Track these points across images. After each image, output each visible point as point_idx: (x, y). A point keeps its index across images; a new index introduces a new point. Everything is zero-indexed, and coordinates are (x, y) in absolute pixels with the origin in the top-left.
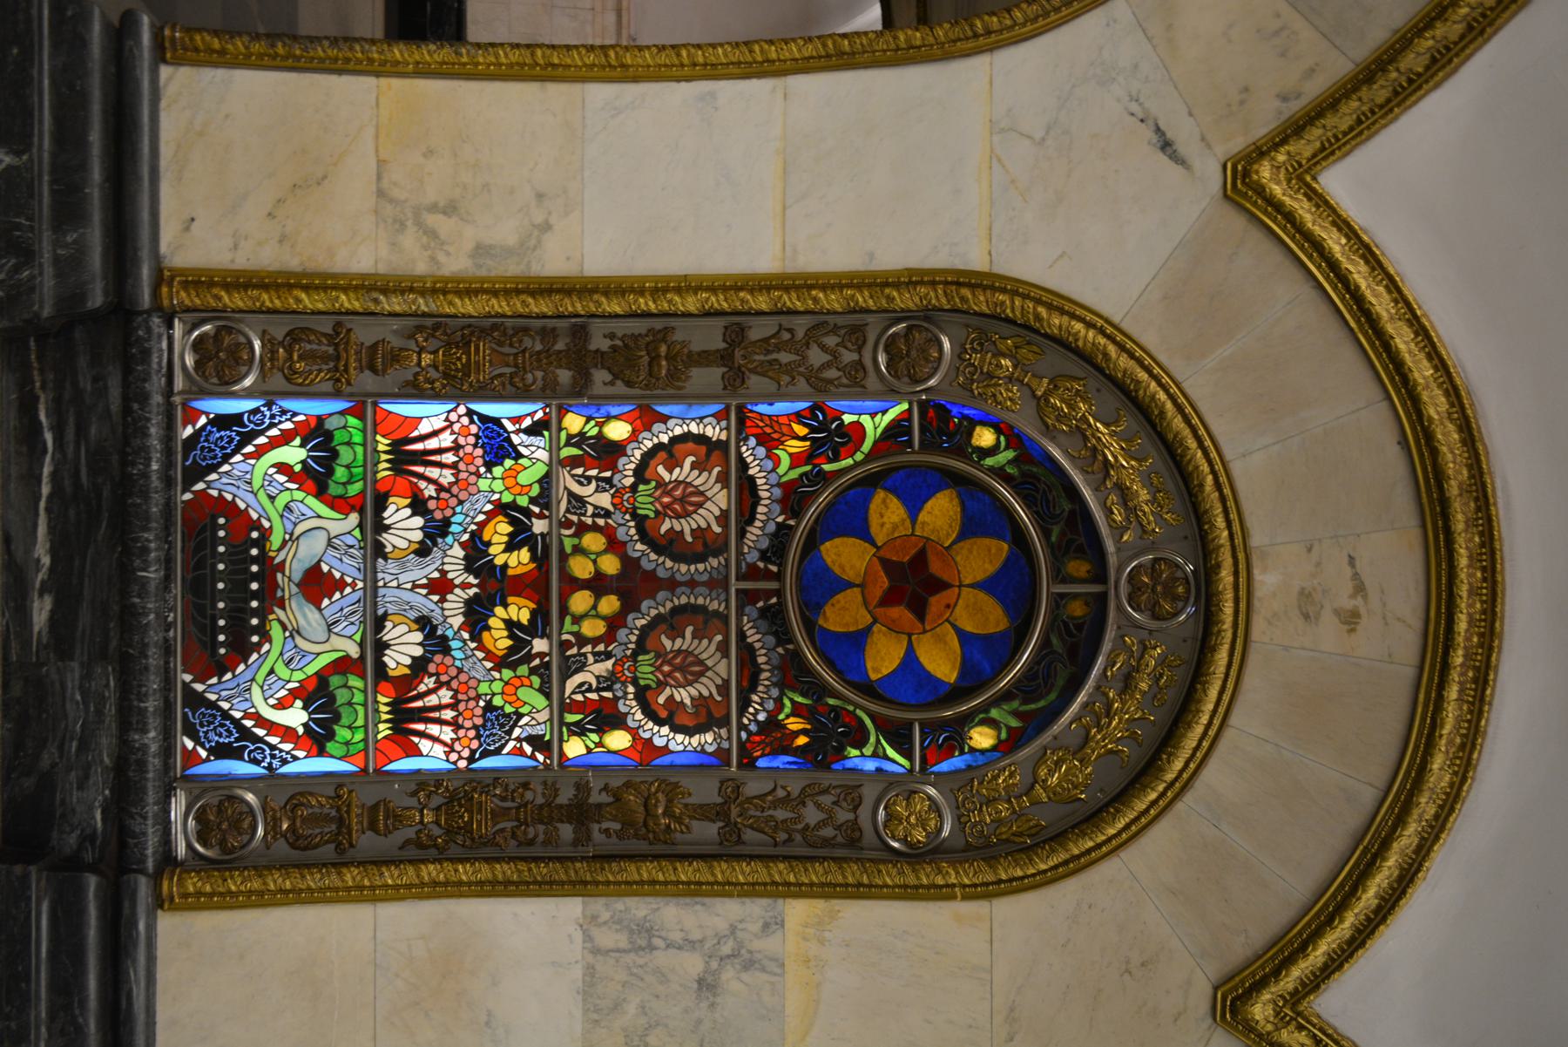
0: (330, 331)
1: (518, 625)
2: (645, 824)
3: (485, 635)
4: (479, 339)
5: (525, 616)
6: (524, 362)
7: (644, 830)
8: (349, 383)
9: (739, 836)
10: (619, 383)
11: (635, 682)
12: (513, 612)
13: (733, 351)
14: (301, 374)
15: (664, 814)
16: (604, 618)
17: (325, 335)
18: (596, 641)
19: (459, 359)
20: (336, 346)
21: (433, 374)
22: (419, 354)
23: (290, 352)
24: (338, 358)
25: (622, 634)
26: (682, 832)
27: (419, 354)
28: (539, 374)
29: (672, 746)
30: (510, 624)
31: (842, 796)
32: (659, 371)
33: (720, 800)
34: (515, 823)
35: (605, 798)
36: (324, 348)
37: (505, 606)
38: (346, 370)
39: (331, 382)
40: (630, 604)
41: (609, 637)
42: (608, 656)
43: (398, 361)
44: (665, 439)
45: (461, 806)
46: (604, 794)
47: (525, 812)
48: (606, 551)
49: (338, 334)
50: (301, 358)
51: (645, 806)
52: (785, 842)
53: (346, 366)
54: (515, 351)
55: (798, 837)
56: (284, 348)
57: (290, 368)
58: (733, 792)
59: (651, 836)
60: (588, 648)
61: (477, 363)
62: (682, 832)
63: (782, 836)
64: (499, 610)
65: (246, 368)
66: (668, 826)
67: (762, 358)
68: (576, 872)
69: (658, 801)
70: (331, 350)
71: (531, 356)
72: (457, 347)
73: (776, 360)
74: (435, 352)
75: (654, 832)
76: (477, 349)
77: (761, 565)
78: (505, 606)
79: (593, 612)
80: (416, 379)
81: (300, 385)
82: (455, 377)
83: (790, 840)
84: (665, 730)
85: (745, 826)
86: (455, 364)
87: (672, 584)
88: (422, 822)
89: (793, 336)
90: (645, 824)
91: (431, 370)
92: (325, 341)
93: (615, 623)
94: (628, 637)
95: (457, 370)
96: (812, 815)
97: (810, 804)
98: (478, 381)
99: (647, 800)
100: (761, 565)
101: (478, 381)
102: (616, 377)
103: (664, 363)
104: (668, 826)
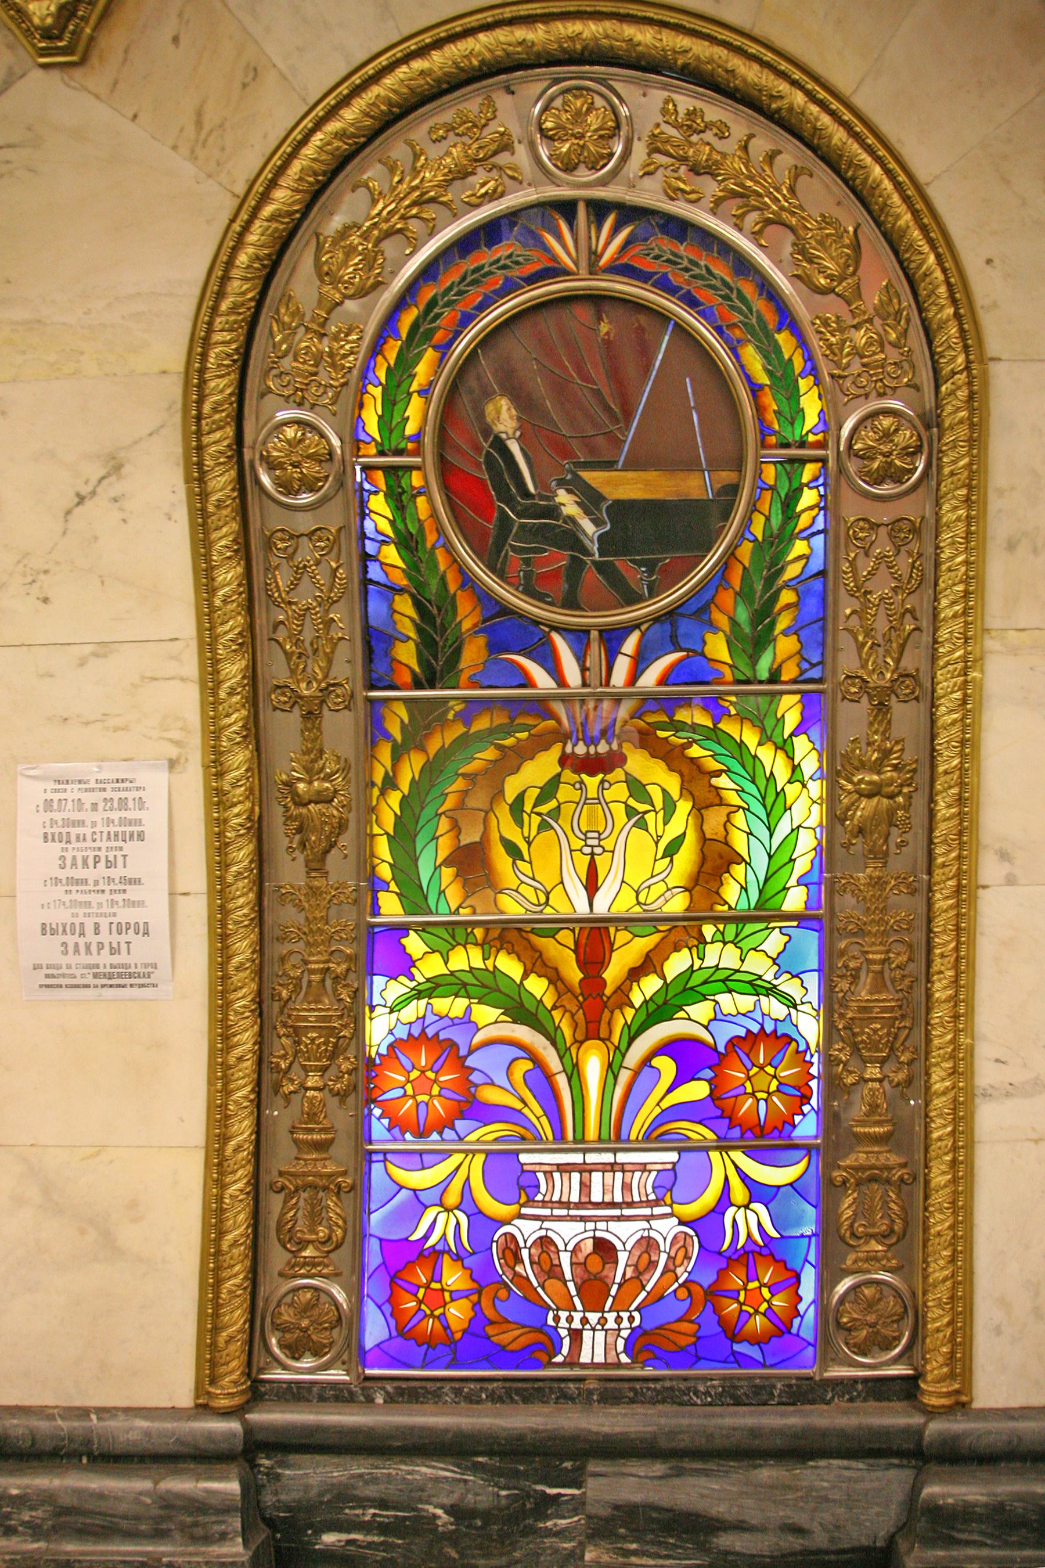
0: (281, 1197)
8: (345, 1173)
14: (332, 1231)
17: (285, 1202)
19: (313, 1040)
20: (297, 1190)
21: (332, 1073)
22: (307, 1089)
24: (314, 1187)
27: (307, 1089)
43: (315, 1114)
45: (864, 1033)
54: (306, 974)
57: (324, 1243)
61: (319, 1019)
67: (309, 662)
73: (312, 644)
76: (305, 1019)
80: (338, 1094)
82: (336, 1045)
86: (319, 1046)
88: (880, 1081)
89: (282, 622)
91: (328, 1074)
92: (294, 1201)
98: (341, 1017)
101: (341, 1017)
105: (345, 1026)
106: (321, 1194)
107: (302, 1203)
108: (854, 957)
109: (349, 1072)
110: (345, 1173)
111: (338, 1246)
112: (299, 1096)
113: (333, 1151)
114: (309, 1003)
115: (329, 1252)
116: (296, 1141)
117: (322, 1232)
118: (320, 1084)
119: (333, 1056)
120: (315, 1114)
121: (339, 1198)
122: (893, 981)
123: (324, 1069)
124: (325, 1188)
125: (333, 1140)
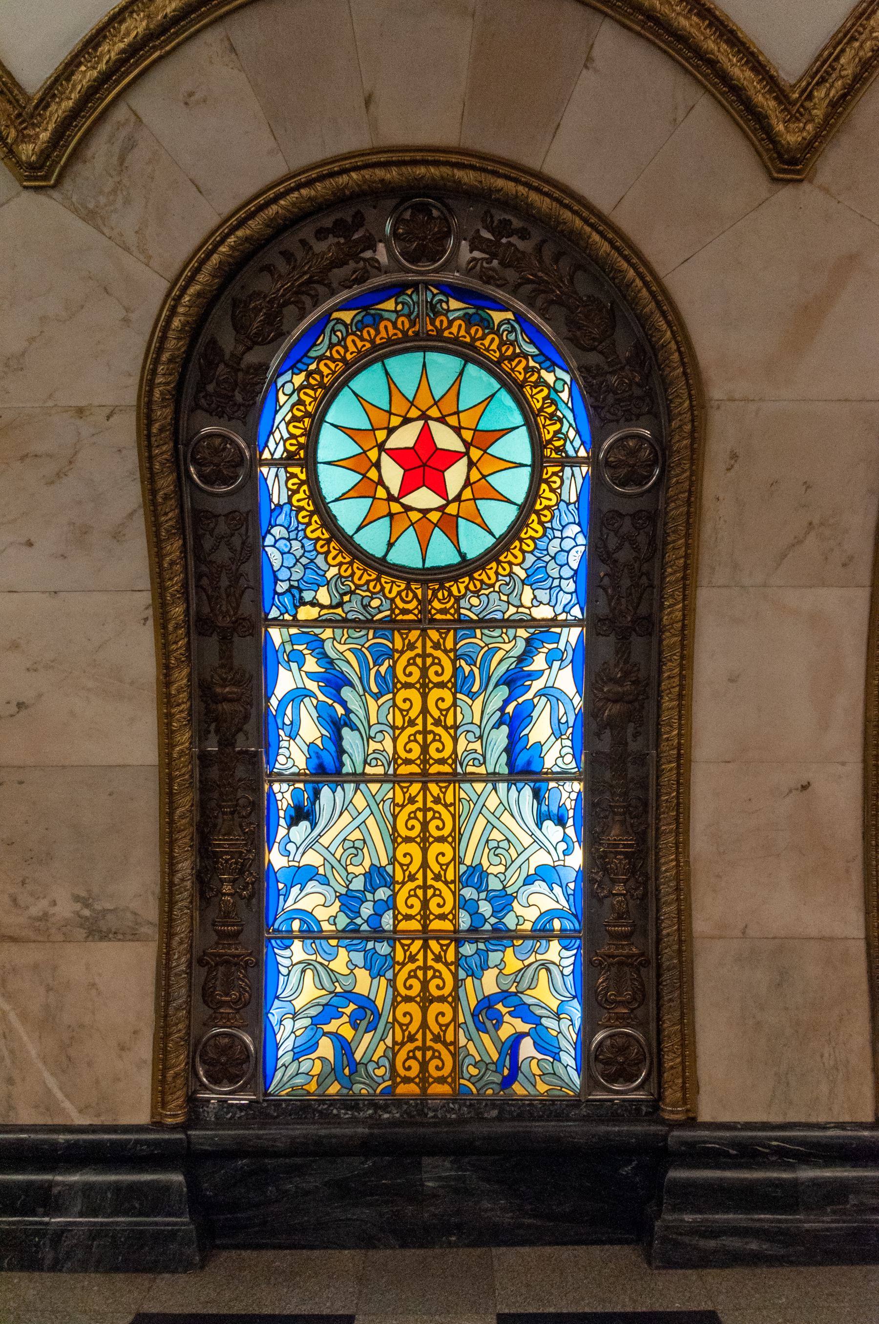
2: (631, 702)
4: (210, 844)
6: (229, 807)
7: (636, 704)
9: (644, 618)
10: (246, 727)
13: (219, 627)
15: (622, 686)
19: (227, 861)
20: (217, 964)
23: (222, 1004)
24: (227, 962)
26: (639, 670)
28: (240, 794)
31: (610, 527)
32: (235, 693)
33: (612, 636)
34: (627, 815)
35: (607, 735)
36: (220, 975)
38: (238, 956)
39: (250, 970)
46: (602, 737)
47: (618, 807)
49: (208, 963)
50: (227, 995)
51: (615, 701)
52: (649, 579)
53: (234, 956)
54: (220, 815)
55: (645, 567)
56: (220, 1007)
57: (234, 1003)
58: (604, 624)
59: (641, 697)
62: (639, 670)
63: (644, 580)
65: (237, 1042)
66: (633, 683)
68: (670, 762)
69: (609, 691)
70: (221, 969)
71: (224, 801)
72: (217, 862)
74: (222, 881)
75: (638, 694)
76: (219, 846)
81: (250, 996)
82: (243, 865)
83: (647, 574)
85: (635, 613)
90: (631, 702)
95: (236, 863)
96: (625, 555)
97: (614, 556)
98: (246, 845)
99: (608, 700)
101: (246, 845)
102: (240, 730)
103: (227, 689)
104: (633, 683)
105: (249, 851)
106: (233, 968)
107: (220, 975)
108: (603, 810)
109: (253, 883)
110: (250, 954)
111: (245, 1005)
112: (216, 899)
113: (242, 937)
114: (224, 835)
115: (240, 1009)
116: (216, 931)
117: (234, 995)
118: (232, 891)
119: (241, 872)
120: (229, 913)
121: (246, 971)
122: (632, 826)
123: (234, 881)
124: (236, 964)
125: (242, 930)
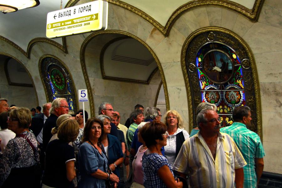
1: (229, 119)
3: (230, 124)
5: (228, 118)
11: (235, 104)
12: (228, 120)
15: (251, 100)
16: (227, 108)
18: (230, 109)
25: (229, 106)
29: (243, 99)
30: (229, 121)
37: (227, 121)
40: (226, 104)
41: (230, 107)
42: (232, 108)
44: (206, 100)
48: (219, 107)
60: (231, 110)
64: (227, 122)
77: (219, 87)
78: (227, 121)
79: (227, 109)
84: (241, 100)
87: (223, 99)
93: (228, 106)
94: (230, 105)
100: (219, 87)
